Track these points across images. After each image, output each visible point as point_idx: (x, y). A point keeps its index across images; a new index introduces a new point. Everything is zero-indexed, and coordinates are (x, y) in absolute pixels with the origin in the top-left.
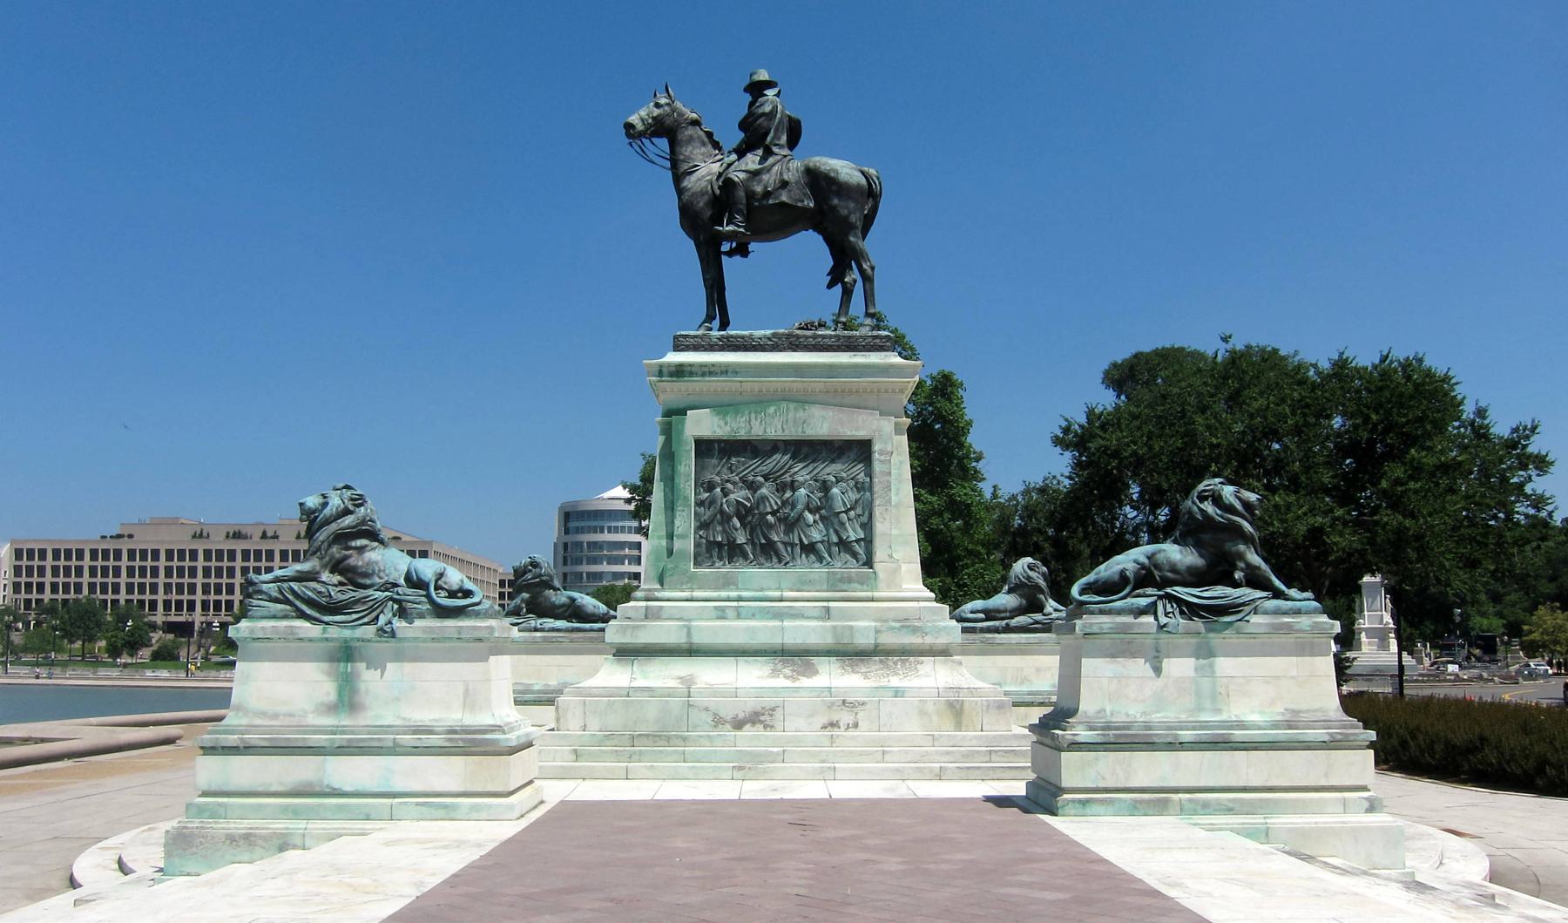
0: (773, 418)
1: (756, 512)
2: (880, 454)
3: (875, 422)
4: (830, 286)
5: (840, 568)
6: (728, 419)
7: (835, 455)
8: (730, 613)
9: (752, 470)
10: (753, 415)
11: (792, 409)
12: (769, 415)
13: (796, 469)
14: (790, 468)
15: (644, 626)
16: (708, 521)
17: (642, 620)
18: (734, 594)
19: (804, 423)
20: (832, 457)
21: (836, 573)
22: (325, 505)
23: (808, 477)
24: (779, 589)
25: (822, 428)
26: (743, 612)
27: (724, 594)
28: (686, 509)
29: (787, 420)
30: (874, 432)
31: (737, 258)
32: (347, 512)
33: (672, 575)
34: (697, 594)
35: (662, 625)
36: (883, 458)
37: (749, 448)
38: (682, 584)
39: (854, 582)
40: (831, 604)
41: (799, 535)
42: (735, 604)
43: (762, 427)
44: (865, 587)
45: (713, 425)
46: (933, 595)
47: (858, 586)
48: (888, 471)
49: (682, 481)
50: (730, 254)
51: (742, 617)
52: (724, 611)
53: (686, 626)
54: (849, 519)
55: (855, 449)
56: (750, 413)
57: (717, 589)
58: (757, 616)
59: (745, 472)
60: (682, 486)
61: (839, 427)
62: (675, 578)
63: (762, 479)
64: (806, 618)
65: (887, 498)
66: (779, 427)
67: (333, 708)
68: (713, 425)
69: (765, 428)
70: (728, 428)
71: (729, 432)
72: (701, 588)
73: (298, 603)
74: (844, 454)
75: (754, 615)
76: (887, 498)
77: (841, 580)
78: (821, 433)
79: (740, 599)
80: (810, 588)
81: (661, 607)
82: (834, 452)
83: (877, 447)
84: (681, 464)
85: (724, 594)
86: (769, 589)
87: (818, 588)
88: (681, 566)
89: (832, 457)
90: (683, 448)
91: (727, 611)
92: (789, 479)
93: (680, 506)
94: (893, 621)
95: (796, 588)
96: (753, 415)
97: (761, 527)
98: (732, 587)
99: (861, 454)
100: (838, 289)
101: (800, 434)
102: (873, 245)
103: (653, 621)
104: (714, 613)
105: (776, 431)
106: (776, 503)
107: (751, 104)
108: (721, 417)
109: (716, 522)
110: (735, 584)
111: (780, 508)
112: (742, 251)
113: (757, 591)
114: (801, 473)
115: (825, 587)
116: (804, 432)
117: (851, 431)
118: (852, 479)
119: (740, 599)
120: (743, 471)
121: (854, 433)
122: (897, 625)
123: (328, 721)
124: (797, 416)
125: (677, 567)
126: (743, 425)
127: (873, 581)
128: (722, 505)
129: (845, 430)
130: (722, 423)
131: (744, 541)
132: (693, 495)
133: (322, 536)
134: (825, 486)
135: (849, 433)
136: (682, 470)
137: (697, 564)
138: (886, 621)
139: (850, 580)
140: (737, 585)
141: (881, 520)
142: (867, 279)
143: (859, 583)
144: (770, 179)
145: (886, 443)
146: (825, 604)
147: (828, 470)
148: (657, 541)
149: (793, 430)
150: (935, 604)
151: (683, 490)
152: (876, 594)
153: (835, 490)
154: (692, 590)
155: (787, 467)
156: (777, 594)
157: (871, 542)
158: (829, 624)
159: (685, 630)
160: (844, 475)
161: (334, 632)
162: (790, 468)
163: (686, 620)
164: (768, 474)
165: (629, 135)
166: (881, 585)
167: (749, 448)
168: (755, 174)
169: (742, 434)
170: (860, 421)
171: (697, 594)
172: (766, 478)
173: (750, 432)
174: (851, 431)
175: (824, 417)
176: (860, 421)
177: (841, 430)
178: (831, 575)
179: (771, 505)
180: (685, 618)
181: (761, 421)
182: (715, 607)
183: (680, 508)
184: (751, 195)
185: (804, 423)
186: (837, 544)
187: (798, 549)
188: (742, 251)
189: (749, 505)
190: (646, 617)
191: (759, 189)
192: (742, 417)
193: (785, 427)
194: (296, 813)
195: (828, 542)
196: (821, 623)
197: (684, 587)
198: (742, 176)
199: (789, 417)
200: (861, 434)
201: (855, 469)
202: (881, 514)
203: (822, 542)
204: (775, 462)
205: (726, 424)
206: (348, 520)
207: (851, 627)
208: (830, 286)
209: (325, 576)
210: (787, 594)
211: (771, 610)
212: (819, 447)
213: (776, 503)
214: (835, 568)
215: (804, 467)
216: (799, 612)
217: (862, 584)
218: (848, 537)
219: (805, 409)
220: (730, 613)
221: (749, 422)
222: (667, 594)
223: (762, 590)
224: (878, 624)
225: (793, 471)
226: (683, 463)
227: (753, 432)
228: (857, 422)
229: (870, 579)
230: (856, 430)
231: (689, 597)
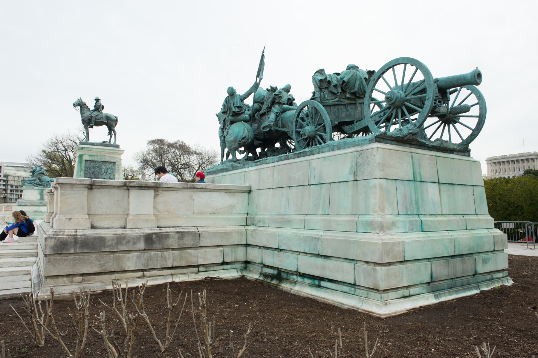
4: (108, 135)
22: (37, 169)
31: (91, 128)
32: (40, 170)
50: (90, 127)
67: (40, 200)
73: (33, 184)
83: (116, 163)
100: (110, 136)
102: (116, 129)
107: (96, 103)
112: (92, 127)
123: (39, 202)
133: (36, 174)
142: (115, 135)
144: (99, 117)
153: (109, 170)
161: (40, 188)
165: (74, 106)
168: (97, 115)
169: (93, 160)
172: (97, 167)
184: (96, 119)
188: (92, 127)
191: (97, 118)
194: (35, 215)
198: (95, 116)
200: (114, 161)
206: (40, 172)
208: (108, 135)
209: (37, 180)
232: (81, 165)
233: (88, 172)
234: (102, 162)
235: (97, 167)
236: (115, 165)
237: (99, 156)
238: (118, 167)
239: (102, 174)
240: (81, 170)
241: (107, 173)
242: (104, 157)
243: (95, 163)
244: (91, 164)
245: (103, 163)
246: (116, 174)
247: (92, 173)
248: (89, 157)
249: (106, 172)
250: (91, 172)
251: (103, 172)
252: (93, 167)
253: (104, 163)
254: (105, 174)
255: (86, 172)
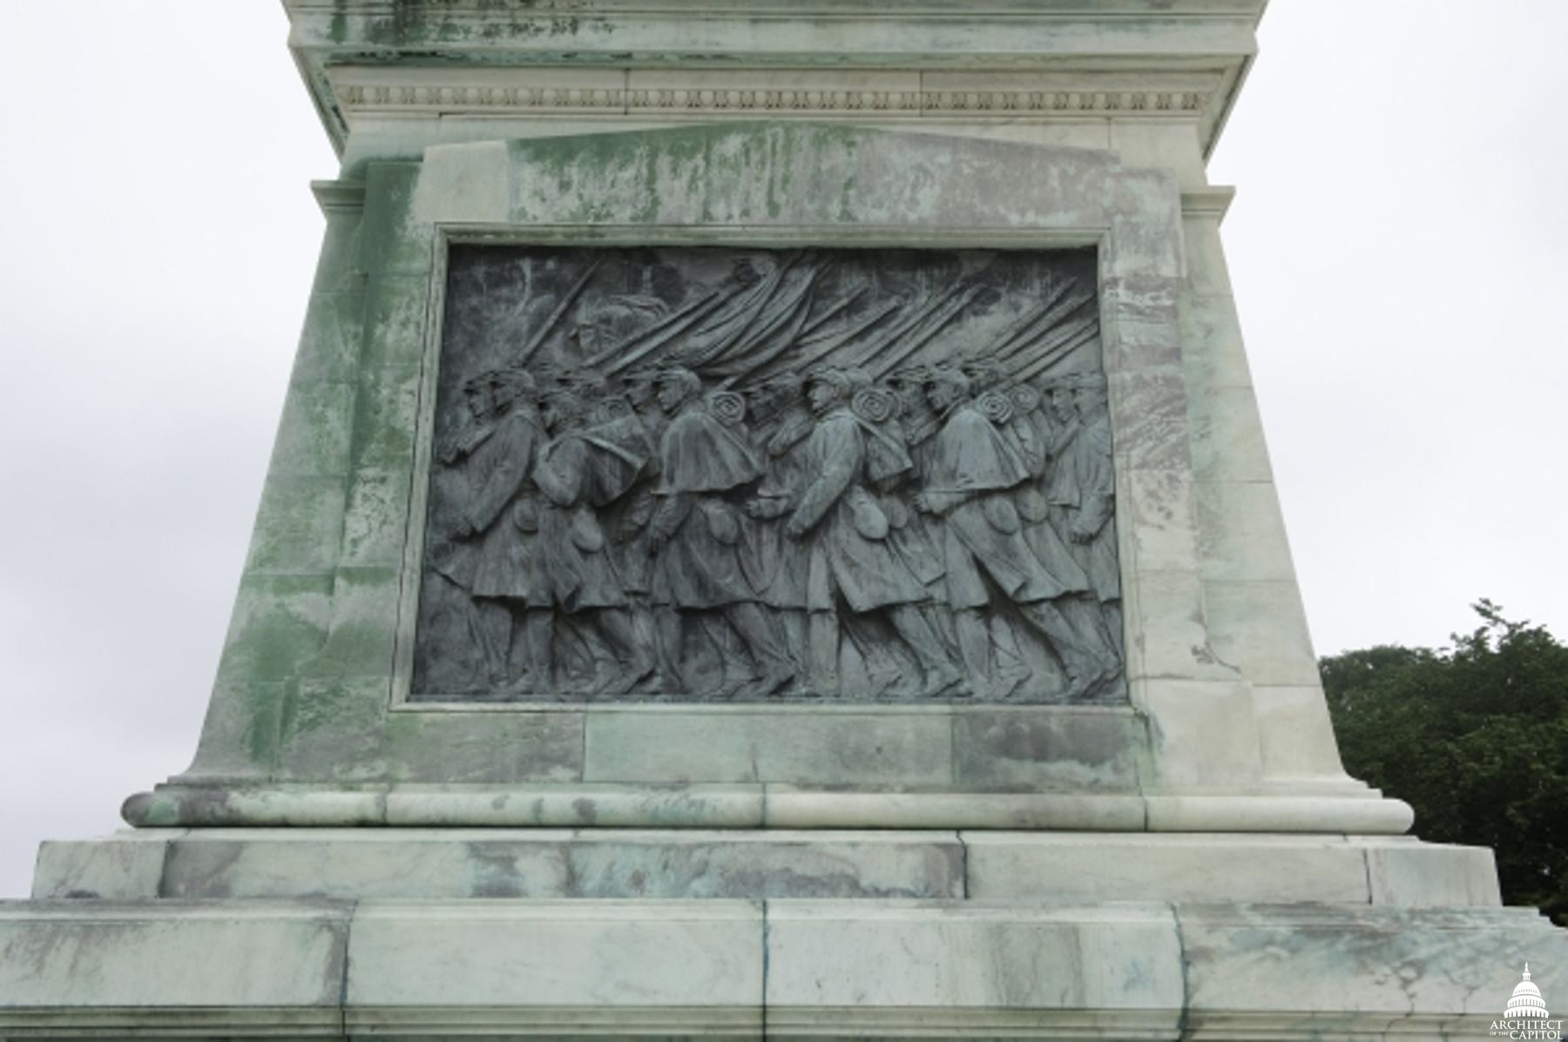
0: (735, 167)
1: (663, 489)
2: (1135, 286)
3: (1109, 183)
5: (998, 702)
6: (573, 172)
7: (965, 299)
8: (536, 870)
9: (654, 351)
10: (664, 162)
11: (805, 143)
12: (723, 162)
13: (822, 349)
14: (796, 344)
15: (133, 924)
16: (480, 527)
17: (141, 903)
18: (559, 800)
19: (848, 185)
20: (954, 306)
21: (990, 721)
23: (865, 376)
24: (750, 779)
25: (914, 202)
26: (594, 865)
27: (519, 801)
28: (394, 475)
29: (786, 180)
30: (1108, 215)
33: (312, 725)
34: (414, 799)
35: (220, 923)
36: (1145, 301)
37: (647, 275)
38: (352, 759)
39: (1063, 755)
40: (969, 838)
41: (832, 576)
42: (566, 835)
43: (702, 194)
44: (1106, 774)
45: (515, 192)
46: (1401, 811)
47: (1083, 772)
48: (1168, 345)
49: (387, 376)
51: (589, 886)
52: (508, 863)
53: (327, 924)
54: (1025, 520)
55: (1037, 284)
56: (653, 155)
57: (493, 778)
58: (655, 885)
59: (629, 358)
60: (385, 392)
61: (977, 201)
62: (322, 735)
63: (692, 377)
64: (865, 894)
65: (1173, 438)
66: (759, 198)
68: (515, 192)
69: (706, 203)
70: (571, 203)
71: (573, 216)
72: (428, 775)
74: (996, 298)
75: (638, 881)
76: (1173, 438)
77: (1009, 746)
78: (912, 217)
79: (586, 821)
80: (872, 779)
81: (240, 846)
82: (960, 291)
84: (385, 318)
85: (519, 801)
86: (713, 781)
87: (911, 778)
88: (357, 688)
89: (954, 306)
90: (401, 266)
91: (523, 864)
92: (792, 381)
93: (375, 461)
94: (1256, 907)
95: (824, 776)
96: (664, 162)
97: (684, 550)
98: (560, 773)
99: (1059, 301)
101: (834, 220)
103: (197, 905)
104: (470, 873)
105: (746, 213)
106: (746, 463)
108: (548, 163)
109: (506, 526)
110: (563, 760)
111: (759, 480)
113: (656, 787)
114: (840, 357)
115: (942, 775)
116: (846, 215)
117: (1022, 212)
118: (1027, 381)
119: (586, 821)
120: (626, 349)
121: (1031, 218)
122: (1282, 928)
124: (825, 166)
125: (336, 692)
126: (627, 193)
127: (1136, 753)
128: (531, 465)
129: (1002, 211)
130: (550, 184)
131: (615, 597)
132: (427, 428)
134: (929, 403)
135: (1014, 219)
136: (390, 339)
137: (417, 690)
138: (1227, 909)
139: (1042, 749)
140: (578, 766)
141: (1156, 517)
143: (1082, 761)
145: (1154, 250)
146: (949, 837)
147: (935, 351)
148: (271, 599)
149: (809, 207)
150: (1415, 843)
151: (385, 409)
152: (1159, 806)
154: (390, 781)
155: (786, 338)
156: (738, 801)
157: (1116, 602)
158: (965, 920)
159: (326, 939)
160: (1003, 368)
162: (796, 344)
163: (335, 902)
164: (716, 361)
166: (1175, 768)
167: (647, 275)
169: (623, 226)
170: (1055, 183)
171: (414, 799)
173: (650, 214)
174: (1022, 212)
175: (919, 168)
176: (1055, 183)
177: (982, 208)
178: (963, 721)
179: (723, 465)
180: (337, 894)
181: (693, 180)
182: (473, 848)
183: (370, 472)
185: (848, 185)
186: (984, 612)
187: (825, 631)
189: (639, 464)
190: (164, 889)
192: (622, 167)
193: (780, 198)
195: (947, 604)
196: (934, 914)
197: (360, 772)
199: (793, 167)
201: (1038, 350)
202: (1151, 494)
203: (922, 605)
204: (743, 321)
205: (565, 186)
207: (1071, 934)
210: (787, 802)
211: (718, 857)
212: (901, 276)
213: (746, 463)
214: (979, 701)
215: (849, 342)
216: (839, 867)
217: (1095, 761)
218: (1023, 586)
219: (852, 144)
220: (536, 870)
221: (651, 181)
222: (279, 801)
223: (681, 784)
224: (1191, 922)
225: (807, 354)
226: (397, 316)
227: (661, 218)
228: (1044, 183)
229: (1122, 743)
230: (1045, 207)
231: (372, 813)
232: (368, 349)
233: (503, 482)
234: (804, 278)
235: (708, 371)
236: (1089, 311)
237: (732, 145)
238: (1159, 334)
239: (802, 519)
240: (360, 438)
241: (934, 498)
242: (838, 157)
243: (669, 289)
244: (585, 314)
245: (813, 296)
246: (1133, 488)
247: (607, 509)
248: (529, 173)
249: (893, 462)
250: (558, 477)
251: (835, 471)
252: (622, 380)
253: (853, 282)
254: (873, 514)
255: (458, 485)
